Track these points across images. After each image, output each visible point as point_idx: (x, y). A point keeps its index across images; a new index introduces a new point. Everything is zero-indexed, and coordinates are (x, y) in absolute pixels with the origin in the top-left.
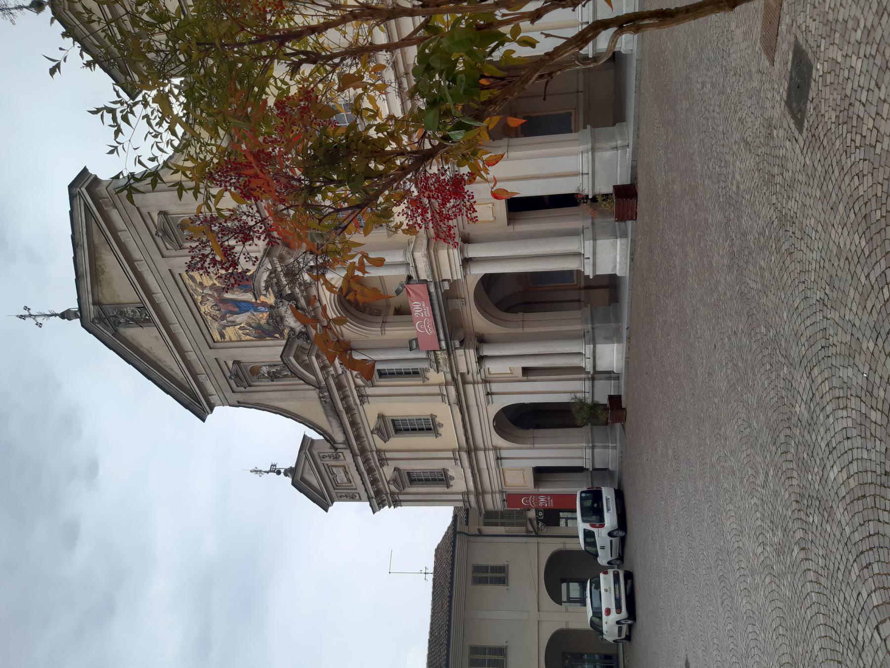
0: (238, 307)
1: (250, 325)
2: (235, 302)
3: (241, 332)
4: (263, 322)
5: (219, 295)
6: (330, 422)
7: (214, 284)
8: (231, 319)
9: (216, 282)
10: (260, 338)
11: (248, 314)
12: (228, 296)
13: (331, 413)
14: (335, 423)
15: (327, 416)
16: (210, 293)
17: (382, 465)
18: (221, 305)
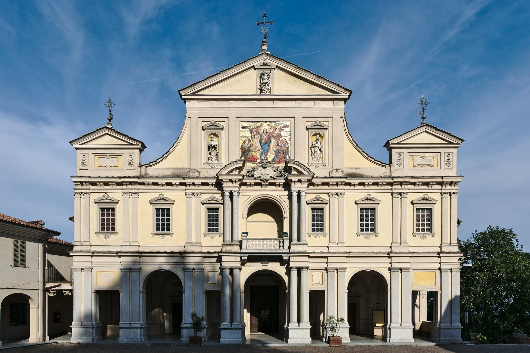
0: (265, 144)
1: (251, 146)
2: (268, 143)
3: (247, 139)
4: (254, 154)
5: (275, 137)
6: (168, 169)
7: (282, 137)
8: (257, 136)
9: (283, 138)
10: (242, 149)
11: (260, 147)
12: (273, 141)
13: (175, 171)
14: (168, 173)
15: (174, 169)
16: (276, 132)
17: (123, 193)
18: (267, 135)
